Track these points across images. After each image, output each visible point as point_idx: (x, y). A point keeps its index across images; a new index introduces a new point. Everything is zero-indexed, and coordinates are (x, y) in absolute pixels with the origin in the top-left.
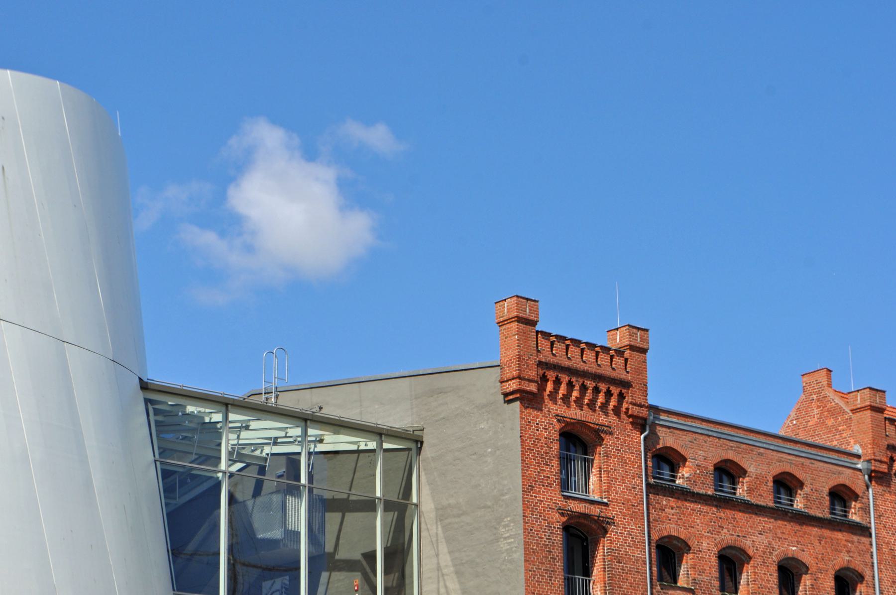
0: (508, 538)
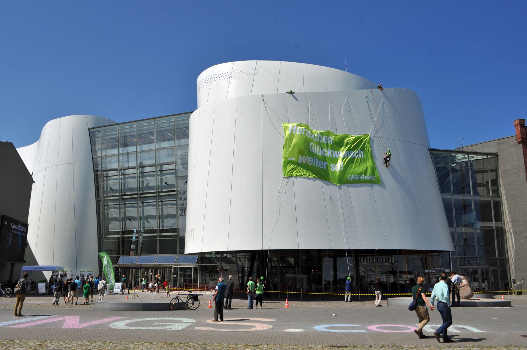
0: (522, 175)
